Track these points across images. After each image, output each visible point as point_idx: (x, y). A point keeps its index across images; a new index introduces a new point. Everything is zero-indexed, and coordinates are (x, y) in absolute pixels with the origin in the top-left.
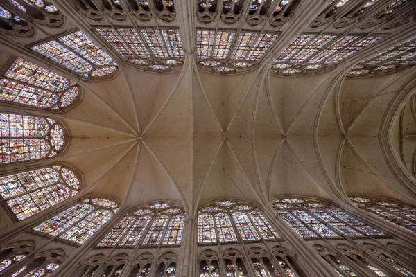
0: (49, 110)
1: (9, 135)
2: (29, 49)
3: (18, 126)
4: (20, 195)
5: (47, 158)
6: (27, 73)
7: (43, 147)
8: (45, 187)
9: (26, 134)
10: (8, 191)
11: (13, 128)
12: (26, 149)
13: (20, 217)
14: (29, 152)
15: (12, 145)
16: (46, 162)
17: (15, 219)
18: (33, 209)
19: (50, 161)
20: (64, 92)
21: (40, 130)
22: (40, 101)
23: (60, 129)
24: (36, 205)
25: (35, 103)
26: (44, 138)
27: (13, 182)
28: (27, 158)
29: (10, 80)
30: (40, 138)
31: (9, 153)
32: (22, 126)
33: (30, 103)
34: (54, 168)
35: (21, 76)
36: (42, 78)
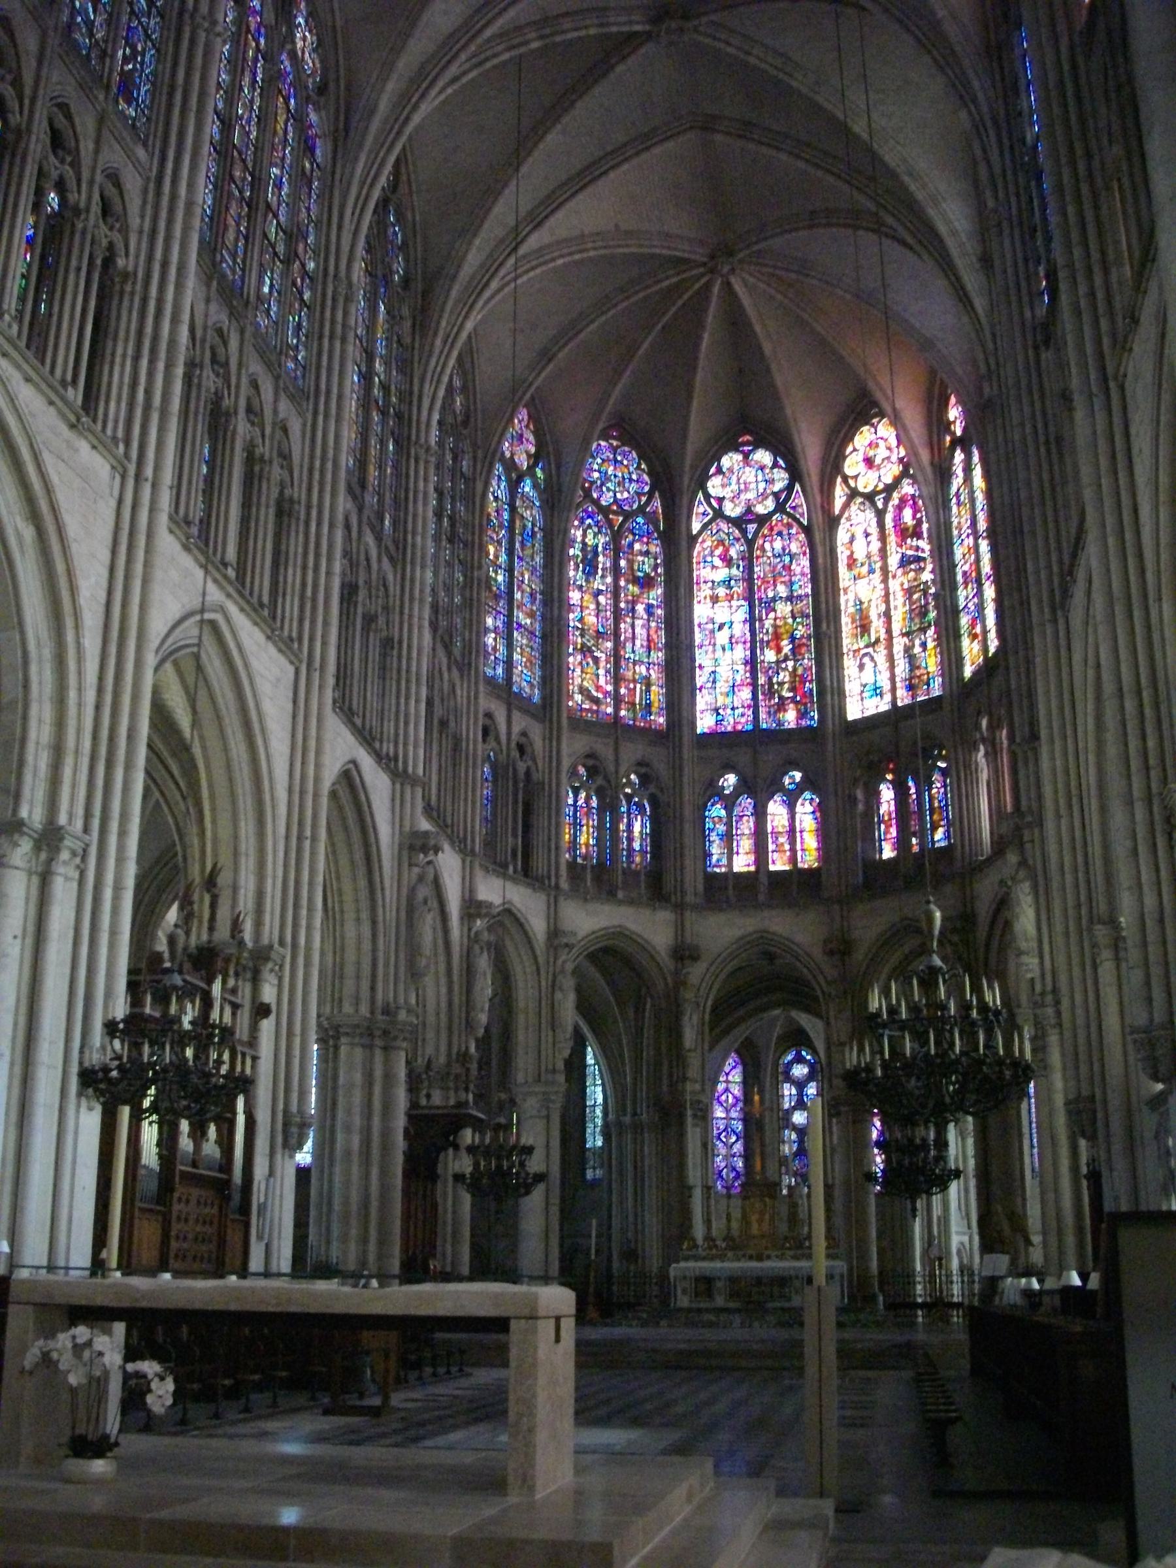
2: (544, 706)
3: (722, 637)
4: (891, 658)
5: (807, 530)
6: (591, 669)
7: (778, 545)
8: (885, 570)
9: (742, 614)
12: (784, 609)
13: (936, 691)
14: (790, 598)
15: (770, 656)
16: (818, 536)
17: (934, 704)
18: (931, 644)
19: (819, 518)
20: (605, 511)
21: (727, 561)
22: (646, 583)
23: (719, 471)
24: (924, 630)
25: (656, 594)
26: (750, 543)
27: (861, 667)
28: (807, 606)
29: (618, 700)
30: (749, 560)
31: (790, 664)
32: (721, 627)
35: (602, 681)
36: (591, 619)
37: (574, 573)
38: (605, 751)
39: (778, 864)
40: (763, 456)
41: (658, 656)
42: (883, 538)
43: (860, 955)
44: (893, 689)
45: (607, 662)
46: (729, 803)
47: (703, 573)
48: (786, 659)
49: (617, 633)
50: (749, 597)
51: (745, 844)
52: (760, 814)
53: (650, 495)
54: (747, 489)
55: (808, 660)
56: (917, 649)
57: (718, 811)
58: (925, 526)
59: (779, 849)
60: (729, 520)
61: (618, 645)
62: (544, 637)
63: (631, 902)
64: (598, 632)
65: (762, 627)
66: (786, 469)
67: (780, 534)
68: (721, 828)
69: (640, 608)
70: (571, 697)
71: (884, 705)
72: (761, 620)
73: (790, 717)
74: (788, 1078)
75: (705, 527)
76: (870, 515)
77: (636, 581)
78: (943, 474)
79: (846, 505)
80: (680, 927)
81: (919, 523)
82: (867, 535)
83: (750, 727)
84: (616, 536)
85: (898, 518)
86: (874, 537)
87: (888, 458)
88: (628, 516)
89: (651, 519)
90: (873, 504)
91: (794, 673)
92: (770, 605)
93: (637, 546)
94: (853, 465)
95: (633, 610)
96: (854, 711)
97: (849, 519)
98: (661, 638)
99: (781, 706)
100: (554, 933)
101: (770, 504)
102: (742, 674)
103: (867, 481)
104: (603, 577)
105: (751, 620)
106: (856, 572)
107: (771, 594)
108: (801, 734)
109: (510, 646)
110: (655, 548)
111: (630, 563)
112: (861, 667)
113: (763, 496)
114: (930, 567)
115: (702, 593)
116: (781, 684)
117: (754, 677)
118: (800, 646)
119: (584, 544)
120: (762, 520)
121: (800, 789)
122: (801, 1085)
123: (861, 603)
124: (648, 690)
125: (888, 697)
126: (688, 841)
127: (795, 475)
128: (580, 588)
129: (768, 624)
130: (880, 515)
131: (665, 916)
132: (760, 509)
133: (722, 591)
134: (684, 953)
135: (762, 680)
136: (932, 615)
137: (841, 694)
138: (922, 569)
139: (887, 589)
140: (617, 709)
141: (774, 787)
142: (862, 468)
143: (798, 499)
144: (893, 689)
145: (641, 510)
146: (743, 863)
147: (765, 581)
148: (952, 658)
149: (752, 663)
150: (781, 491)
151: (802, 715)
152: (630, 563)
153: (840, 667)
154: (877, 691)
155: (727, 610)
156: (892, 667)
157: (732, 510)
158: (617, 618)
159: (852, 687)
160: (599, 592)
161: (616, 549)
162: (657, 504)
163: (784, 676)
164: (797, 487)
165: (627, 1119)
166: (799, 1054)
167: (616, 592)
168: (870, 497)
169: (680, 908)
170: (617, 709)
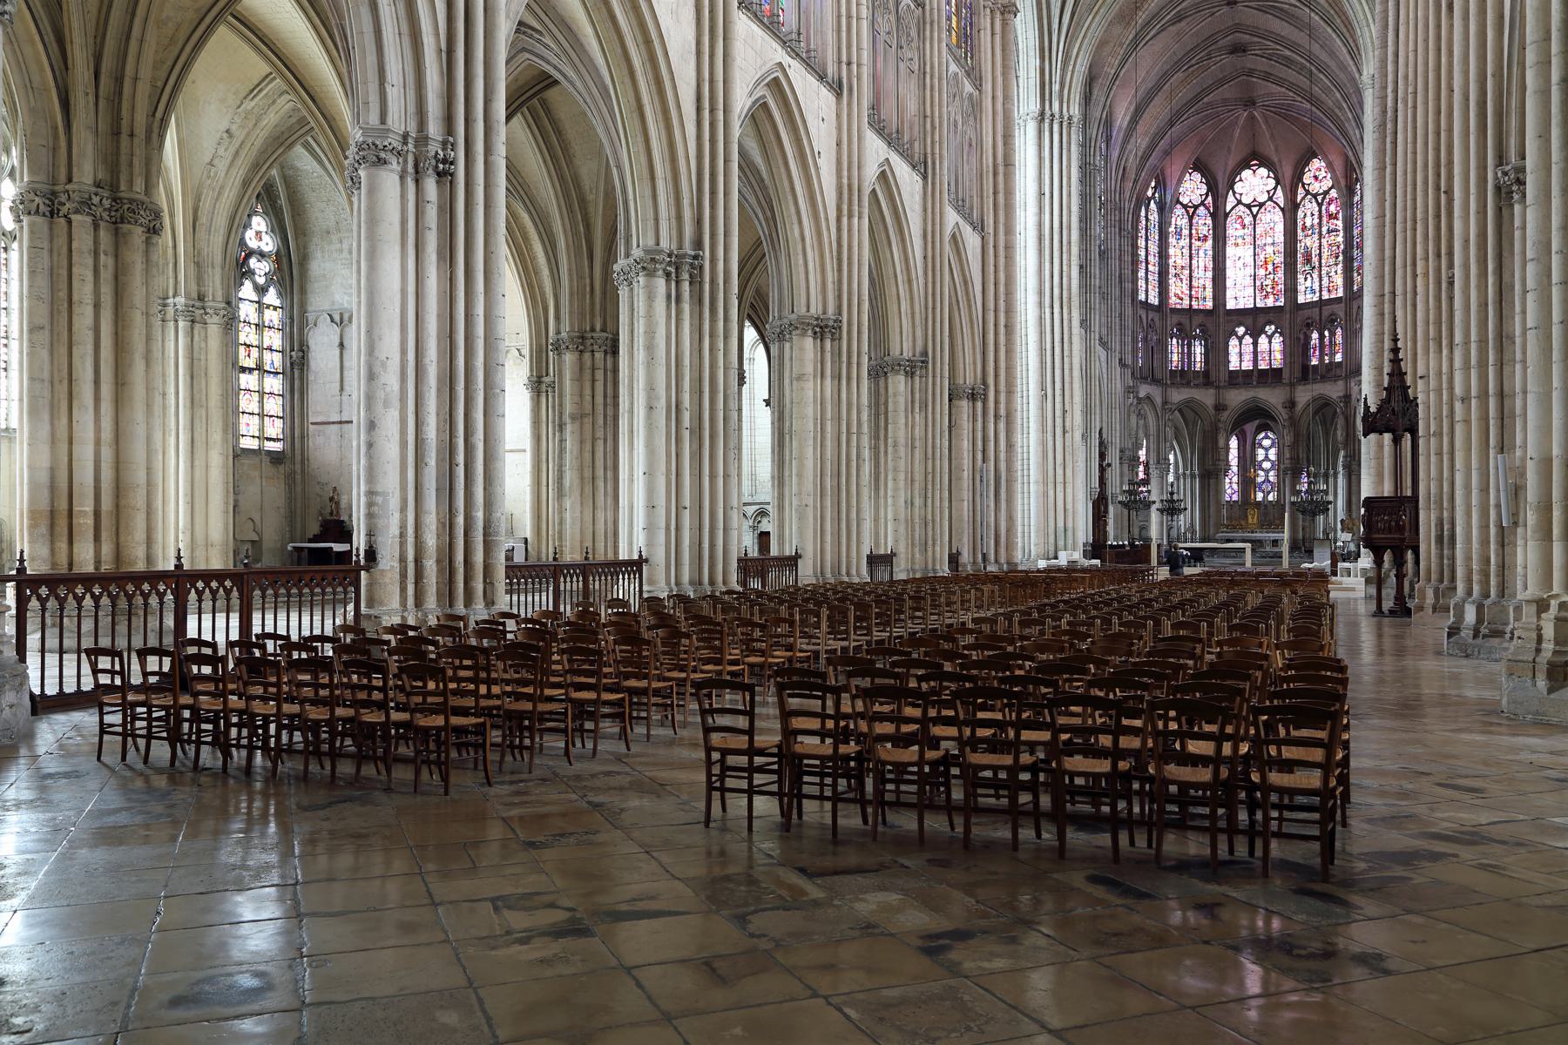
0: (1214, 216)
3: (1239, 264)
5: (1282, 209)
10: (1313, 292)
12: (1270, 249)
13: (1340, 294)
15: (1262, 272)
17: (1338, 300)
18: (1339, 272)
20: (1185, 207)
21: (1244, 227)
22: (1205, 239)
25: (1210, 242)
26: (1255, 217)
27: (1306, 279)
29: (1191, 297)
33: (1210, 253)
37: (1172, 240)
38: (1186, 321)
39: (1263, 366)
40: (1263, 171)
41: (1210, 274)
42: (1320, 217)
43: (1299, 407)
44: (1321, 291)
46: (1240, 339)
47: (1230, 232)
51: (1248, 357)
52: (1255, 344)
53: (1207, 195)
55: (1281, 274)
56: (1332, 274)
58: (1340, 215)
59: (1263, 360)
60: (1245, 205)
62: (1160, 274)
63: (1197, 386)
68: (1237, 350)
69: (1201, 253)
70: (1168, 297)
71: (1315, 299)
73: (1270, 302)
74: (1261, 446)
76: (1315, 204)
79: (1303, 198)
80: (1217, 397)
84: (1191, 219)
85: (1327, 210)
86: (1316, 217)
88: (1196, 207)
89: (1207, 209)
94: (1307, 179)
96: (1301, 299)
98: (1210, 266)
99: (1266, 297)
100: (1165, 403)
102: (1249, 281)
103: (1316, 187)
110: (1209, 221)
112: (1306, 279)
114: (1341, 234)
115: (1230, 242)
120: (1261, 205)
121: (1274, 333)
122: (1267, 450)
126: (1222, 359)
127: (1278, 183)
129: (1262, 257)
130: (1320, 205)
131: (1212, 391)
133: (1240, 241)
134: (1219, 407)
135: (1258, 283)
136: (1341, 258)
137: (1296, 291)
141: (1263, 331)
142: (1313, 180)
143: (1279, 191)
144: (1321, 291)
145: (1202, 203)
146: (1247, 365)
153: (1296, 279)
156: (1321, 280)
157: (1246, 200)
159: (1301, 288)
161: (1191, 225)
162: (1210, 198)
163: (1269, 282)
165: (1188, 472)
168: (1315, 196)
169: (1218, 387)
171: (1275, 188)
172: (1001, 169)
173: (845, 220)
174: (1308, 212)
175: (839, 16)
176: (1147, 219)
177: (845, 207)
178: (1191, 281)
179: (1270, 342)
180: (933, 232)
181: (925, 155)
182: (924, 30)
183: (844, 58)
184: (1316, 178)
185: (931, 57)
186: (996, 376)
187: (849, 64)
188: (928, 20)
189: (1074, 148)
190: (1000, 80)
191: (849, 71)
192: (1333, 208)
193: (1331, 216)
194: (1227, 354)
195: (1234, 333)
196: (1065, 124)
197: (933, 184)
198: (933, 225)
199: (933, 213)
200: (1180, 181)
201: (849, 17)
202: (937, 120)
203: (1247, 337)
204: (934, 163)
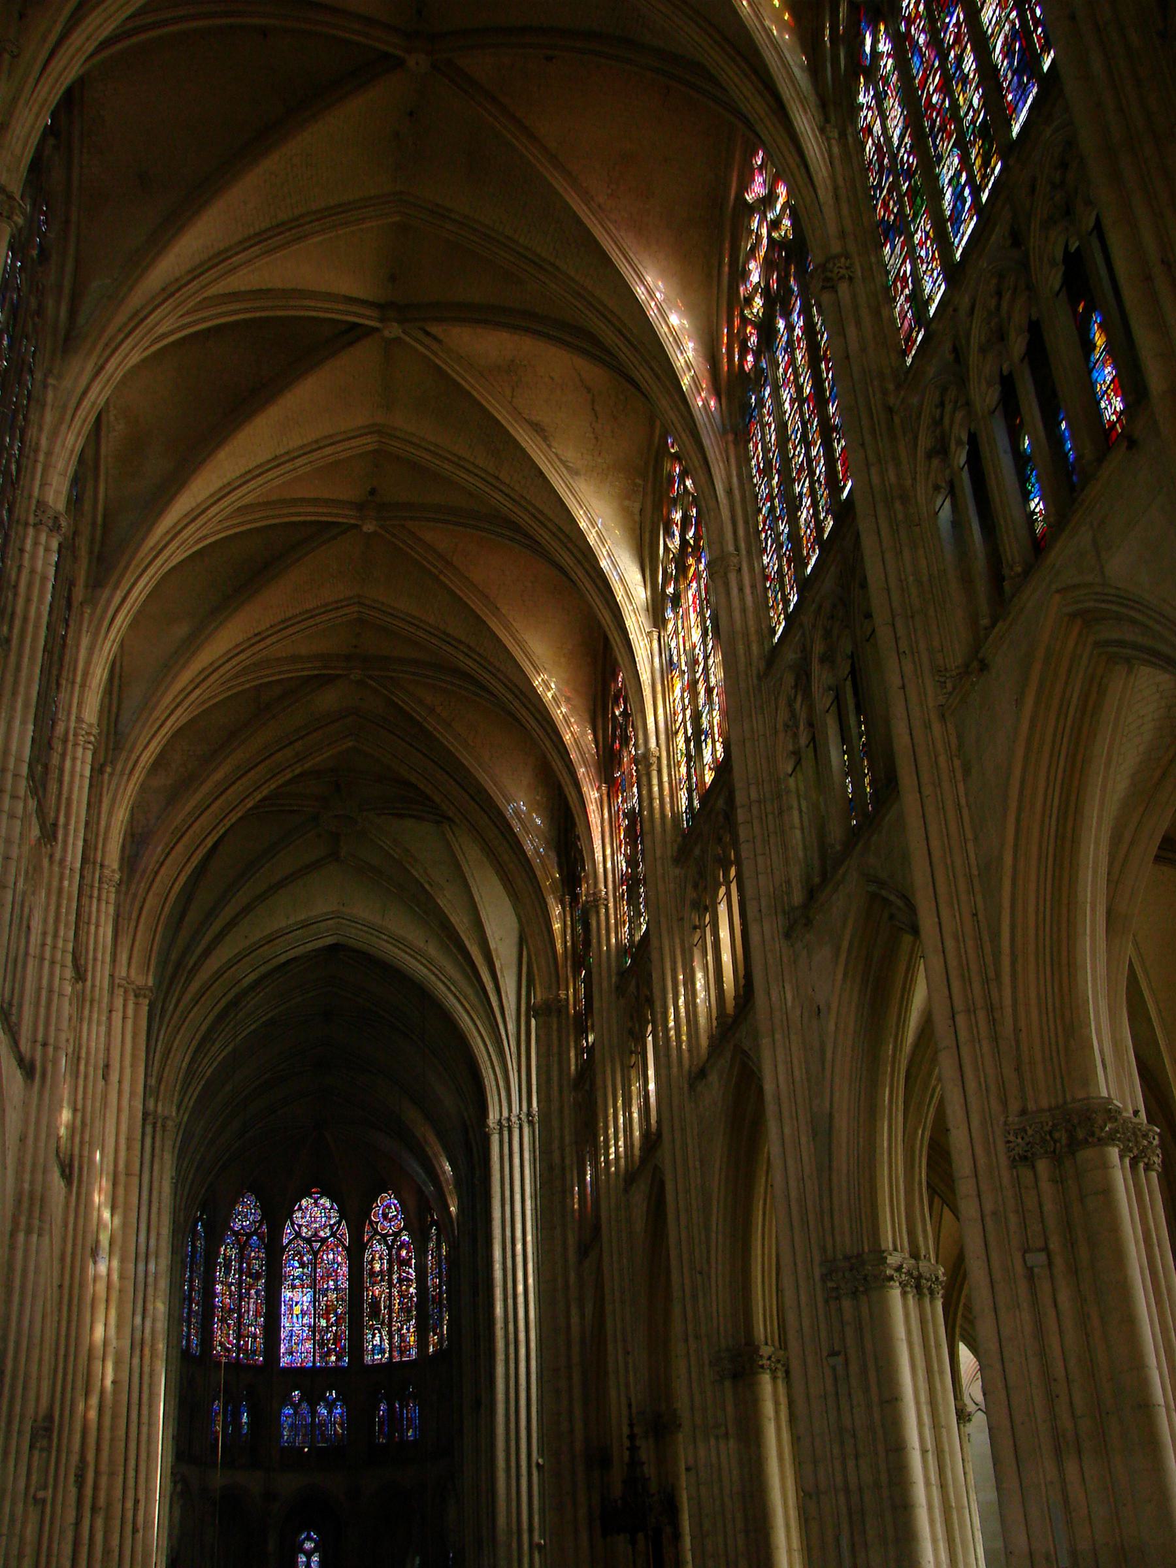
1: (310, 1326)
3: (297, 1310)
4: (390, 1333)
7: (331, 1256)
10: (382, 1351)
11: (300, 1320)
15: (323, 1323)
20: (236, 1233)
21: (302, 1265)
22: (257, 1276)
24: (409, 1321)
26: (315, 1254)
27: (374, 1335)
29: (238, 1346)
30: (314, 1264)
31: (334, 1328)
32: (297, 1303)
34: (368, 1241)
40: (326, 1202)
42: (390, 1262)
44: (390, 1352)
45: (234, 1326)
48: (332, 1325)
49: (240, 1307)
50: (313, 1286)
52: (314, 1413)
53: (261, 1222)
54: (315, 1221)
56: (404, 1331)
57: (288, 1410)
58: (414, 1261)
60: (304, 1239)
61: (240, 1316)
64: (230, 1308)
65: (319, 1305)
66: (338, 1211)
67: (332, 1250)
68: (290, 1420)
69: (253, 1291)
72: (319, 1302)
75: (290, 1242)
77: (250, 1275)
78: (427, 1239)
81: (411, 1258)
82: (381, 1258)
83: (311, 1364)
87: (395, 1216)
88: (249, 1236)
89: (261, 1238)
90: (386, 1243)
91: (336, 1334)
92: (325, 1292)
93: (253, 1254)
95: (249, 1294)
97: (371, 1247)
99: (328, 1354)
101: (327, 1230)
104: (234, 1275)
105: (314, 1300)
106: (373, 1279)
107: (325, 1286)
108: (337, 1370)
109: (189, 1328)
111: (249, 1265)
113: (325, 1226)
114: (414, 1286)
116: (328, 1340)
117: (315, 1336)
118: (341, 1318)
119: (224, 1254)
120: (324, 1241)
122: (309, 1555)
123: (376, 1298)
124: (255, 1341)
125: (387, 1355)
127: (343, 1215)
128: (222, 1282)
130: (390, 1248)
132: (322, 1234)
133: (297, 1282)
138: (409, 1286)
139: (390, 1293)
140: (238, 1355)
143: (344, 1228)
145: (255, 1233)
147: (322, 1277)
148: (422, 1342)
149: (313, 1328)
150: (335, 1224)
151: (339, 1359)
152: (249, 1265)
154: (382, 1351)
155: (300, 1294)
158: (241, 1299)
160: (232, 1284)
161: (241, 1257)
162: (265, 1228)
164: (344, 1222)
166: (309, 1534)
167: (240, 1283)
168: (384, 1236)
170: (238, 1355)
171: (339, 1222)
172: (122, 1178)
173: (21, 1237)
174: (377, 1257)
175: (39, 989)
176: (194, 1246)
177: (23, 1219)
178: (239, 1329)
179: (330, 1412)
180: (73, 1254)
181: (72, 1155)
182: (83, 1008)
183: (40, 1037)
184: (385, 1216)
185: (88, 1040)
186: (98, 1449)
187: (45, 1045)
188: (88, 997)
189: (168, 1157)
190: (128, 1071)
191: (45, 1054)
192: (404, 1253)
193: (405, 1263)
194: (279, 1426)
195: (286, 1399)
196: (159, 1125)
197: (78, 1194)
198: (74, 1245)
199: (75, 1229)
200: (236, 1202)
201: (51, 991)
202: (88, 1115)
203: (304, 1405)
204: (81, 1169)
